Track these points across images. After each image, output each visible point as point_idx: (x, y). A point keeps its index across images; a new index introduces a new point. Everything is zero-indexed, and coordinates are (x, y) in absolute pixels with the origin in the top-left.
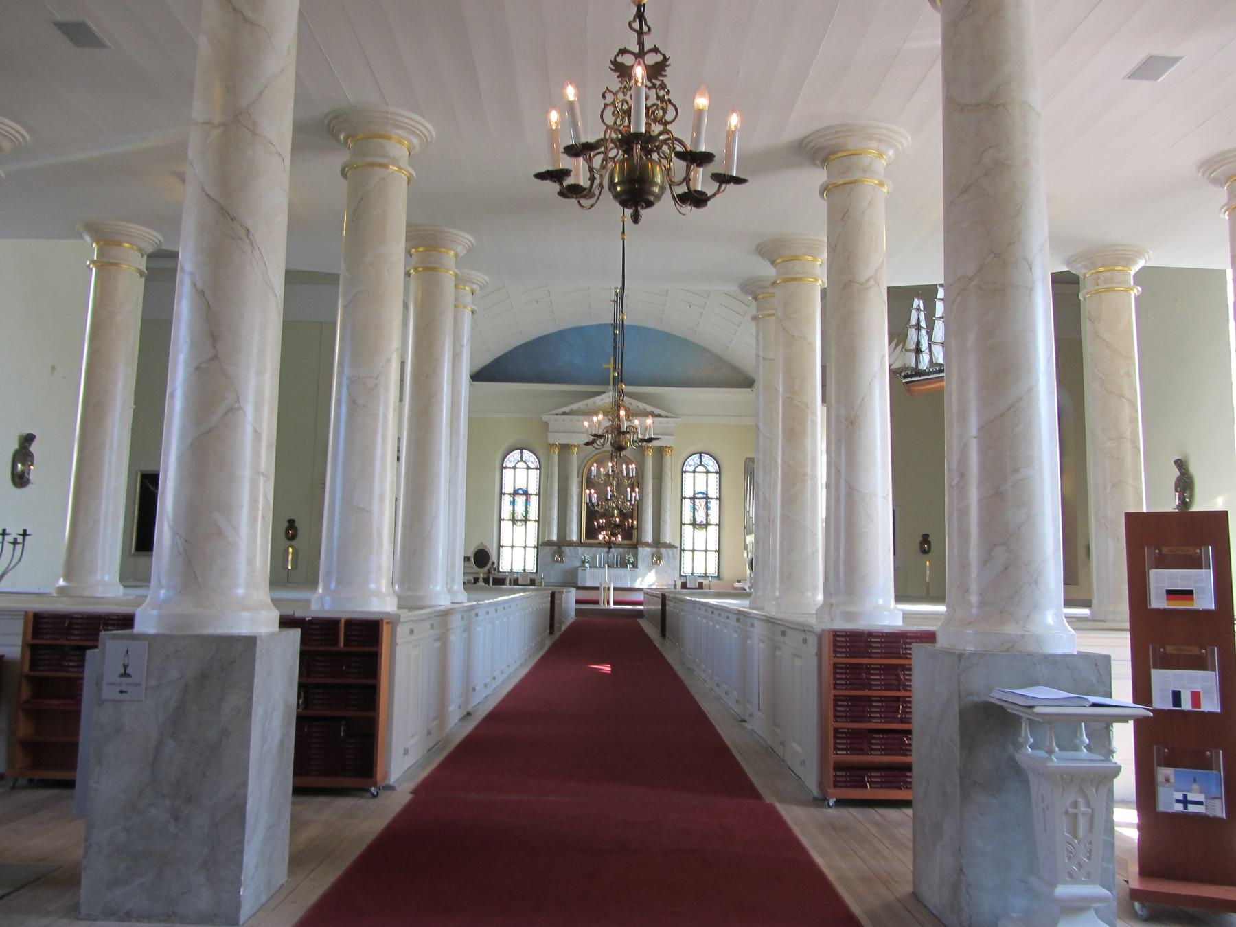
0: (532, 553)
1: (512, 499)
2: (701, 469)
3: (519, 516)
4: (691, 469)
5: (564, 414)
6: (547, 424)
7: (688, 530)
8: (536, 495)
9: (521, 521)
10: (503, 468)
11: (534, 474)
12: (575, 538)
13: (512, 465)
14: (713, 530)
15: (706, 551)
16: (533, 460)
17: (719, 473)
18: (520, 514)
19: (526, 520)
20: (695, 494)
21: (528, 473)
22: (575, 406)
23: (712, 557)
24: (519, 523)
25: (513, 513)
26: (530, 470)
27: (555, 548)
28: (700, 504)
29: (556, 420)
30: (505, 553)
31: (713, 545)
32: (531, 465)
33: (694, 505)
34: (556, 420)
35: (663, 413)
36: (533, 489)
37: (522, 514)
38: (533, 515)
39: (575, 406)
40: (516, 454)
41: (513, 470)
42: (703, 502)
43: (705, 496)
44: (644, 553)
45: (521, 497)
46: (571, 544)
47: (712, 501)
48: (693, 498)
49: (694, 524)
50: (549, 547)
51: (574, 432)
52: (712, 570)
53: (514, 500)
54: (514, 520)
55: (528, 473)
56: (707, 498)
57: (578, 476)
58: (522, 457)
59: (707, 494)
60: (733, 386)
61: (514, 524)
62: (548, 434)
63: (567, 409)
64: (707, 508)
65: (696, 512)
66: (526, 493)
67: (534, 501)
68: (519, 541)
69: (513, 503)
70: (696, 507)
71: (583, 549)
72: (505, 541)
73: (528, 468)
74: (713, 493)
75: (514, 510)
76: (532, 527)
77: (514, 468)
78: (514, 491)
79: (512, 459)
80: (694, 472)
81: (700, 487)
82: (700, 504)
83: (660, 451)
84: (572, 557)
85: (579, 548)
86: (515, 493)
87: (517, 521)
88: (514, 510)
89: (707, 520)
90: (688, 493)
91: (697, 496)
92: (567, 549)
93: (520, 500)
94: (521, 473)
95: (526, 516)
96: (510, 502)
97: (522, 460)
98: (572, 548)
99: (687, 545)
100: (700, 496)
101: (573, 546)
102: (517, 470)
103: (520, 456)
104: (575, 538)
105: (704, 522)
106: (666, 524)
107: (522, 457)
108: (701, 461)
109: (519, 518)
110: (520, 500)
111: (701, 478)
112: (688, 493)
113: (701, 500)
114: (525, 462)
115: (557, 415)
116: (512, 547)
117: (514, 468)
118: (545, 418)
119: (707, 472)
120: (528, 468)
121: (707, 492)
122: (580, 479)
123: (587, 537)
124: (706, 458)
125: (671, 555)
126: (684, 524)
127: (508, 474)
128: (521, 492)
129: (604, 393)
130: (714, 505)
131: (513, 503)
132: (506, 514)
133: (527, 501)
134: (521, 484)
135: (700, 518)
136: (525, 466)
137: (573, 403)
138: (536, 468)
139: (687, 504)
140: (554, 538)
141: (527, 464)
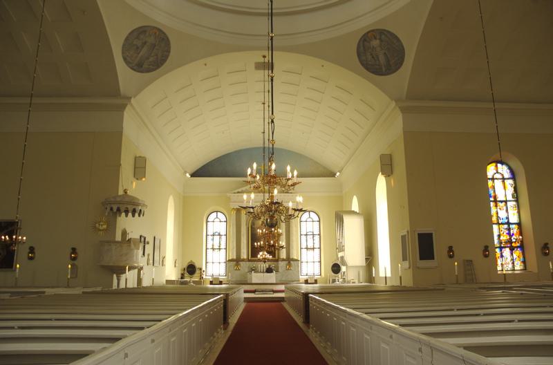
2: (310, 219)
3: (216, 246)
5: (238, 192)
6: (229, 198)
7: (304, 251)
12: (245, 257)
14: (317, 251)
22: (244, 189)
27: (235, 263)
36: (223, 232)
38: (223, 246)
42: (312, 236)
44: (282, 264)
46: (243, 260)
49: (307, 248)
54: (213, 249)
60: (325, 177)
63: (240, 190)
67: (224, 238)
74: (316, 232)
76: (223, 251)
84: (244, 266)
90: (304, 232)
92: (241, 263)
99: (304, 259)
104: (245, 257)
112: (304, 232)
123: (252, 256)
130: (317, 238)
132: (210, 246)
135: (310, 245)
139: (304, 238)
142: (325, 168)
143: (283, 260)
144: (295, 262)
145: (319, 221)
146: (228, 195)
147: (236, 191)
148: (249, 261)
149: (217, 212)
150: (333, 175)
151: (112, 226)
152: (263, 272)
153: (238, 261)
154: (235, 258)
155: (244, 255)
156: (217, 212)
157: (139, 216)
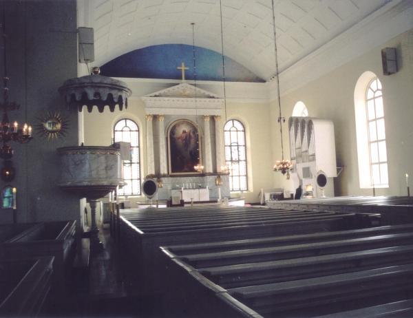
5: (156, 96)
12: (166, 172)
14: (242, 164)
17: (244, 131)
22: (162, 92)
24: (127, 165)
28: (234, 148)
35: (215, 95)
39: (162, 92)
42: (236, 147)
46: (164, 176)
48: (231, 146)
49: (232, 161)
51: (162, 108)
52: (243, 187)
63: (157, 93)
74: (241, 142)
77: (122, 131)
82: (234, 148)
83: (213, 118)
84: (165, 185)
92: (163, 179)
104: (166, 172)
111: (234, 134)
112: (228, 143)
117: (122, 131)
119: (237, 131)
120: (130, 131)
123: (172, 172)
124: (236, 122)
129: (178, 84)
130: (242, 149)
135: (235, 157)
137: (159, 90)
142: (250, 72)
143: (210, 174)
144: (225, 177)
145: (244, 131)
146: (144, 98)
148: (171, 176)
149: (126, 119)
150: (263, 81)
151: (70, 126)
152: (189, 189)
154: (153, 173)
156: (126, 119)
157: (121, 109)
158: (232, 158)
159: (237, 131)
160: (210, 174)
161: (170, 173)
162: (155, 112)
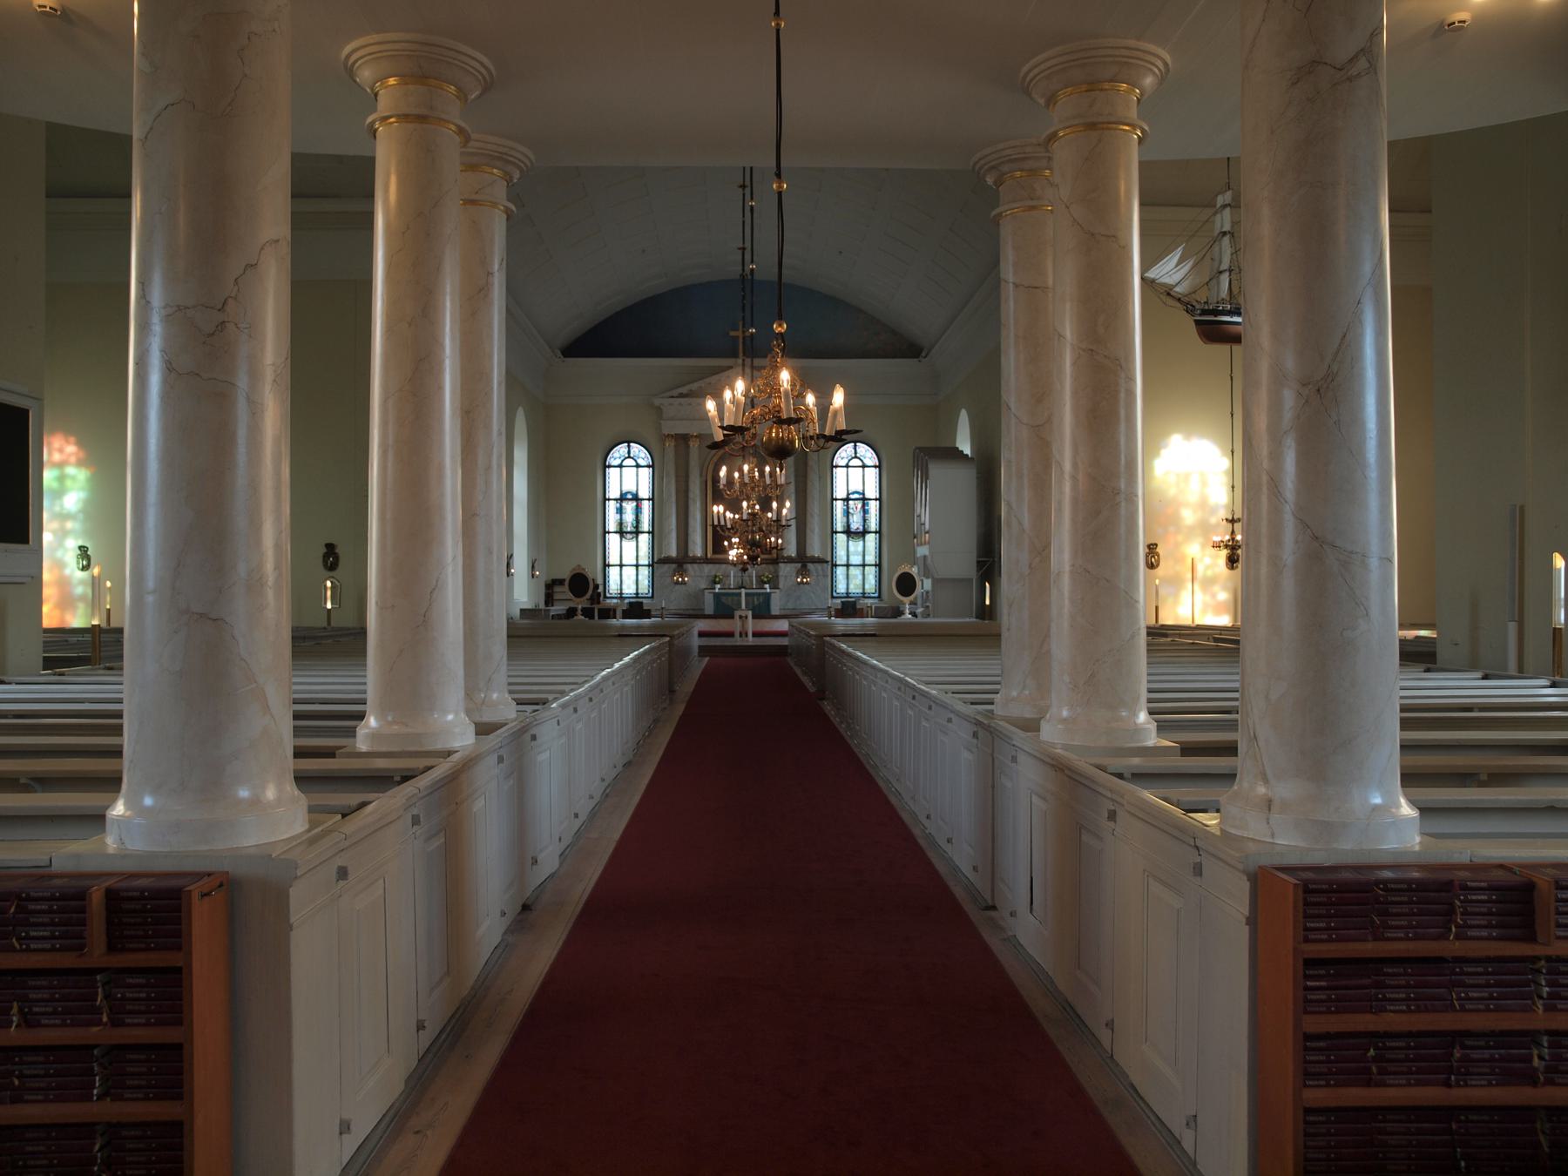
0: (645, 573)
1: (618, 505)
2: (856, 462)
4: (843, 463)
5: (681, 396)
6: (659, 410)
7: (841, 539)
8: (649, 500)
9: (631, 533)
10: (605, 467)
11: (646, 474)
12: (699, 553)
13: (617, 462)
15: (864, 565)
16: (643, 455)
18: (630, 525)
19: (637, 532)
20: (848, 494)
21: (637, 472)
23: (871, 573)
24: (629, 536)
25: (621, 524)
26: (640, 469)
27: (674, 566)
29: (671, 404)
30: (613, 573)
31: (871, 558)
32: (641, 462)
33: (848, 508)
34: (671, 404)
36: (645, 493)
37: (632, 524)
38: (646, 525)
40: (621, 450)
41: (619, 469)
42: (859, 504)
43: (861, 496)
45: (630, 502)
46: (695, 560)
47: (870, 502)
48: (847, 500)
49: (848, 532)
50: (667, 566)
53: (621, 505)
54: (621, 532)
55: (637, 472)
56: (864, 500)
57: (701, 475)
58: (629, 452)
59: (863, 494)
60: (894, 357)
61: (622, 537)
62: (662, 422)
63: (684, 390)
64: (865, 511)
65: (850, 517)
66: (636, 498)
67: (646, 507)
68: (629, 558)
69: (620, 511)
70: (851, 511)
71: (711, 566)
72: (613, 558)
73: (638, 466)
75: (621, 519)
76: (644, 539)
77: (620, 466)
78: (621, 495)
79: (616, 455)
80: (847, 466)
81: (856, 485)
82: (855, 506)
85: (704, 565)
86: (622, 498)
87: (627, 533)
88: (621, 519)
89: (864, 526)
91: (851, 496)
92: (689, 567)
93: (629, 507)
94: (629, 473)
95: (637, 527)
96: (617, 509)
97: (629, 457)
98: (695, 565)
99: (841, 557)
100: (856, 496)
101: (696, 563)
102: (624, 469)
103: (626, 450)
104: (699, 553)
105: (861, 529)
106: (813, 532)
107: (629, 452)
108: (856, 453)
109: (629, 530)
110: (629, 507)
113: (856, 502)
114: (632, 458)
115: (672, 397)
116: (621, 566)
117: (620, 466)
118: (657, 402)
119: (864, 466)
120: (638, 466)
121: (864, 491)
122: (704, 478)
123: (715, 552)
125: (821, 573)
126: (836, 532)
127: (613, 474)
128: (630, 496)
129: (731, 367)
131: (620, 511)
132: (612, 525)
133: (638, 511)
134: (629, 486)
135: (856, 524)
136: (634, 464)
138: (648, 466)
140: (673, 553)
141: (636, 461)
143: (790, 560)
144: (819, 566)
147: (675, 392)
153: (682, 562)
155: (697, 550)
156: (629, 442)
158: (848, 525)
159: (864, 466)
160: (790, 560)
161: (709, 555)
162: (681, 428)
